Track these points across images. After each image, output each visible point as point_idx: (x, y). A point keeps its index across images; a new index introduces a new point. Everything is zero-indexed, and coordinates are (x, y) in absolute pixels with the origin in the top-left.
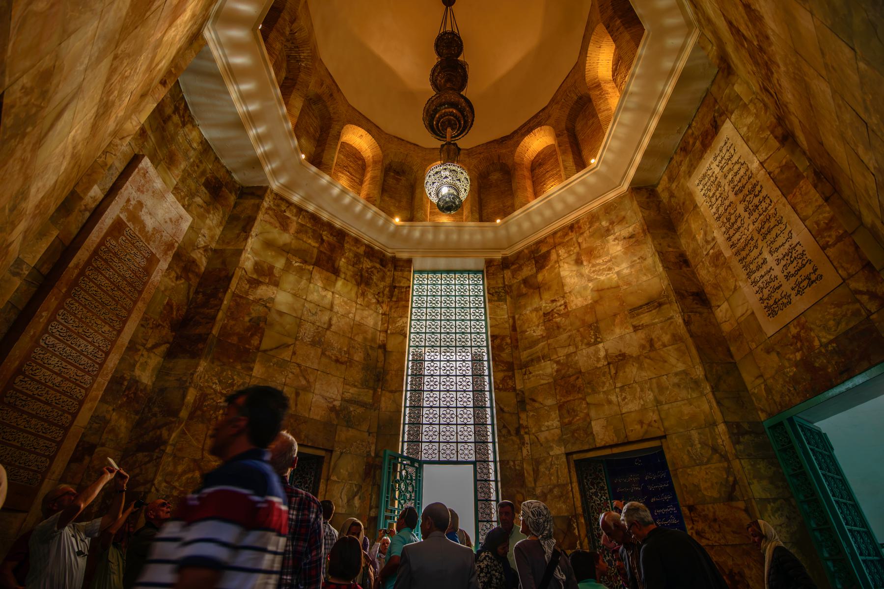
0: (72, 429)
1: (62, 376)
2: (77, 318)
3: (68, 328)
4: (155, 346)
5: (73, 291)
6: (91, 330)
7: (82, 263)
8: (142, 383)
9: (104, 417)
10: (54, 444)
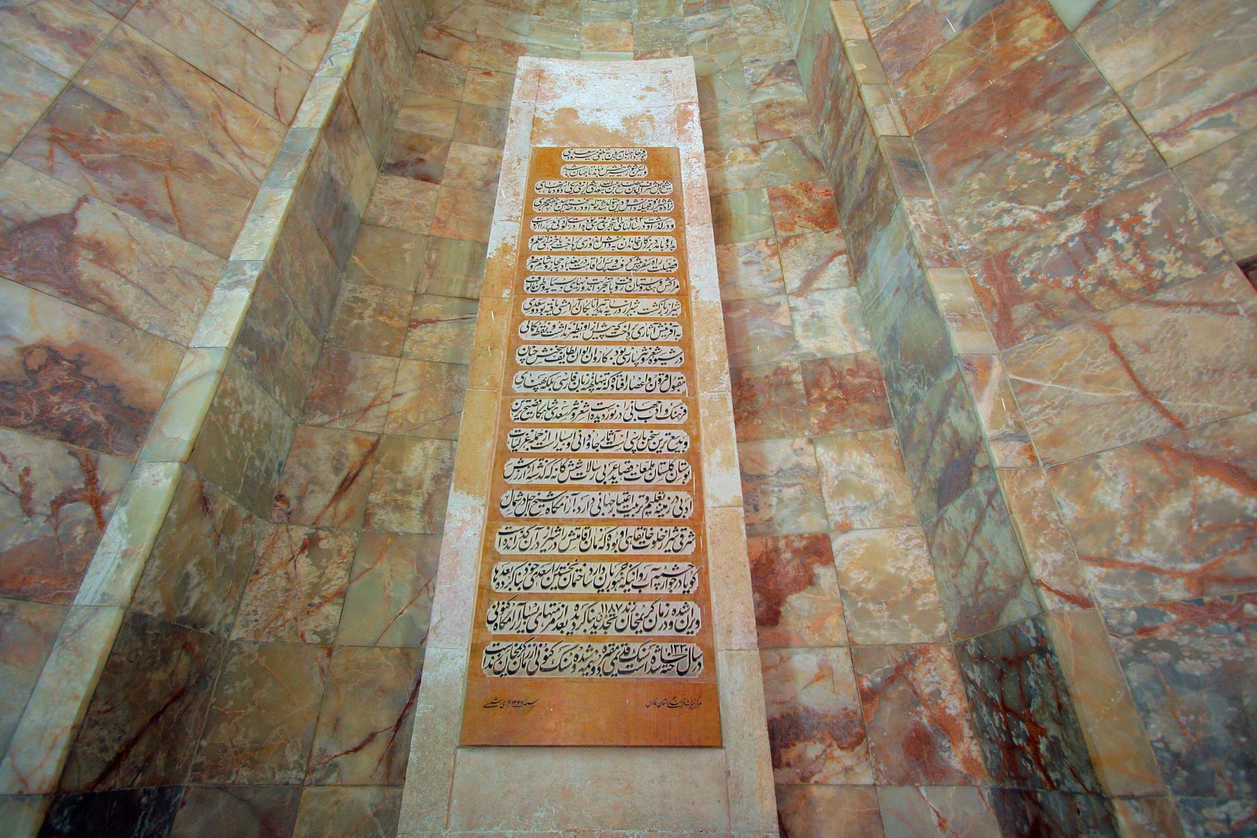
0: (709, 519)
1: (604, 426)
2: (565, 318)
3: (560, 342)
4: (809, 279)
5: (526, 285)
6: (609, 324)
8: (840, 359)
9: (799, 465)
10: (683, 566)
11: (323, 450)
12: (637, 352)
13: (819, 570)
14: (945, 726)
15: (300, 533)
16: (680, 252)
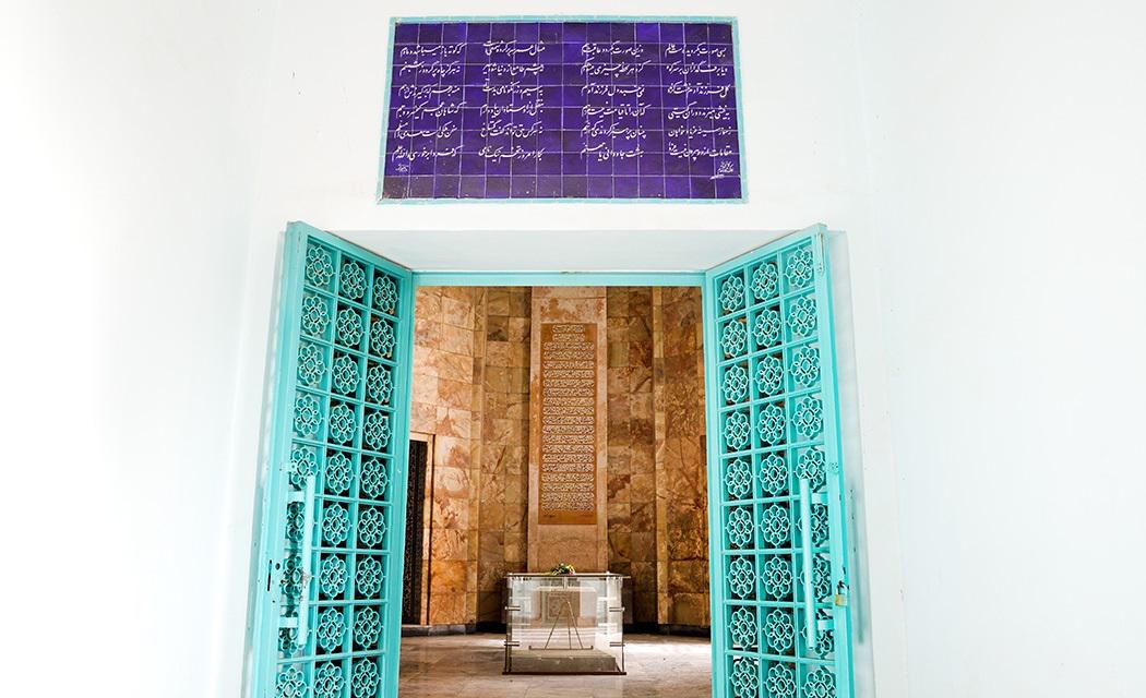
7: (538, 374)
11: (492, 452)
12: (579, 419)
13: (627, 485)
14: (648, 521)
15: (491, 476)
16: (595, 378)
